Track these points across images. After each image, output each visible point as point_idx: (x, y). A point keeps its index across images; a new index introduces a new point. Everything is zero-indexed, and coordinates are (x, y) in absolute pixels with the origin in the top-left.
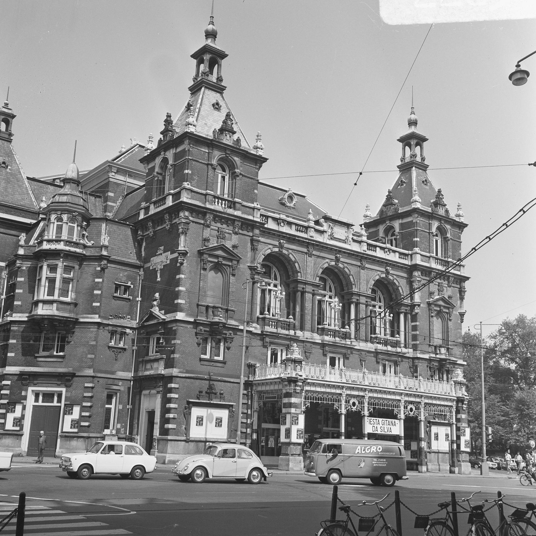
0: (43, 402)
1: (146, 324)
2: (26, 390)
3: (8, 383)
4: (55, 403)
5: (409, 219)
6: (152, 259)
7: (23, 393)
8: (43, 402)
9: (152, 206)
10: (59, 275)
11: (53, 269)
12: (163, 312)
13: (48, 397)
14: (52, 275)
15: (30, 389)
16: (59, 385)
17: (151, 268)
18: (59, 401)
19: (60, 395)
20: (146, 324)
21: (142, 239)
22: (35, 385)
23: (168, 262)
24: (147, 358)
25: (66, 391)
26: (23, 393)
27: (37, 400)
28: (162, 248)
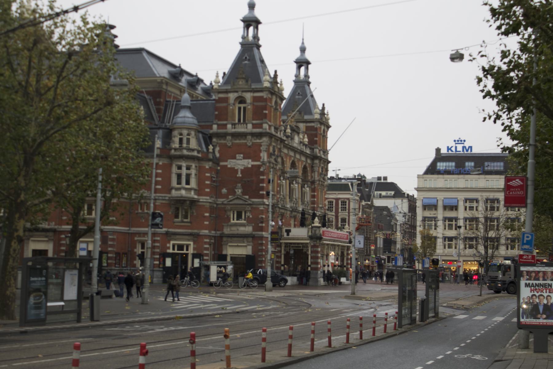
0: (178, 250)
1: (231, 203)
2: (169, 243)
3: (159, 239)
4: (185, 251)
5: (312, 124)
6: (229, 160)
7: (168, 245)
8: (178, 250)
9: (229, 126)
10: (193, 172)
11: (188, 168)
12: (247, 197)
13: (181, 247)
14: (188, 172)
15: (172, 242)
16: (189, 240)
17: (229, 166)
18: (187, 250)
19: (188, 246)
20: (231, 203)
21: (216, 145)
22: (175, 240)
23: (250, 166)
24: (230, 224)
25: (194, 244)
26: (168, 245)
27: (174, 249)
28: (242, 155)
